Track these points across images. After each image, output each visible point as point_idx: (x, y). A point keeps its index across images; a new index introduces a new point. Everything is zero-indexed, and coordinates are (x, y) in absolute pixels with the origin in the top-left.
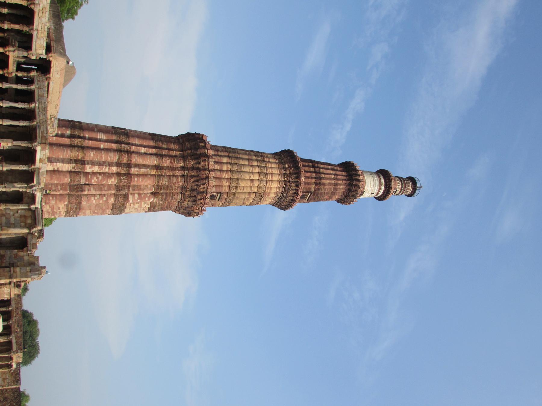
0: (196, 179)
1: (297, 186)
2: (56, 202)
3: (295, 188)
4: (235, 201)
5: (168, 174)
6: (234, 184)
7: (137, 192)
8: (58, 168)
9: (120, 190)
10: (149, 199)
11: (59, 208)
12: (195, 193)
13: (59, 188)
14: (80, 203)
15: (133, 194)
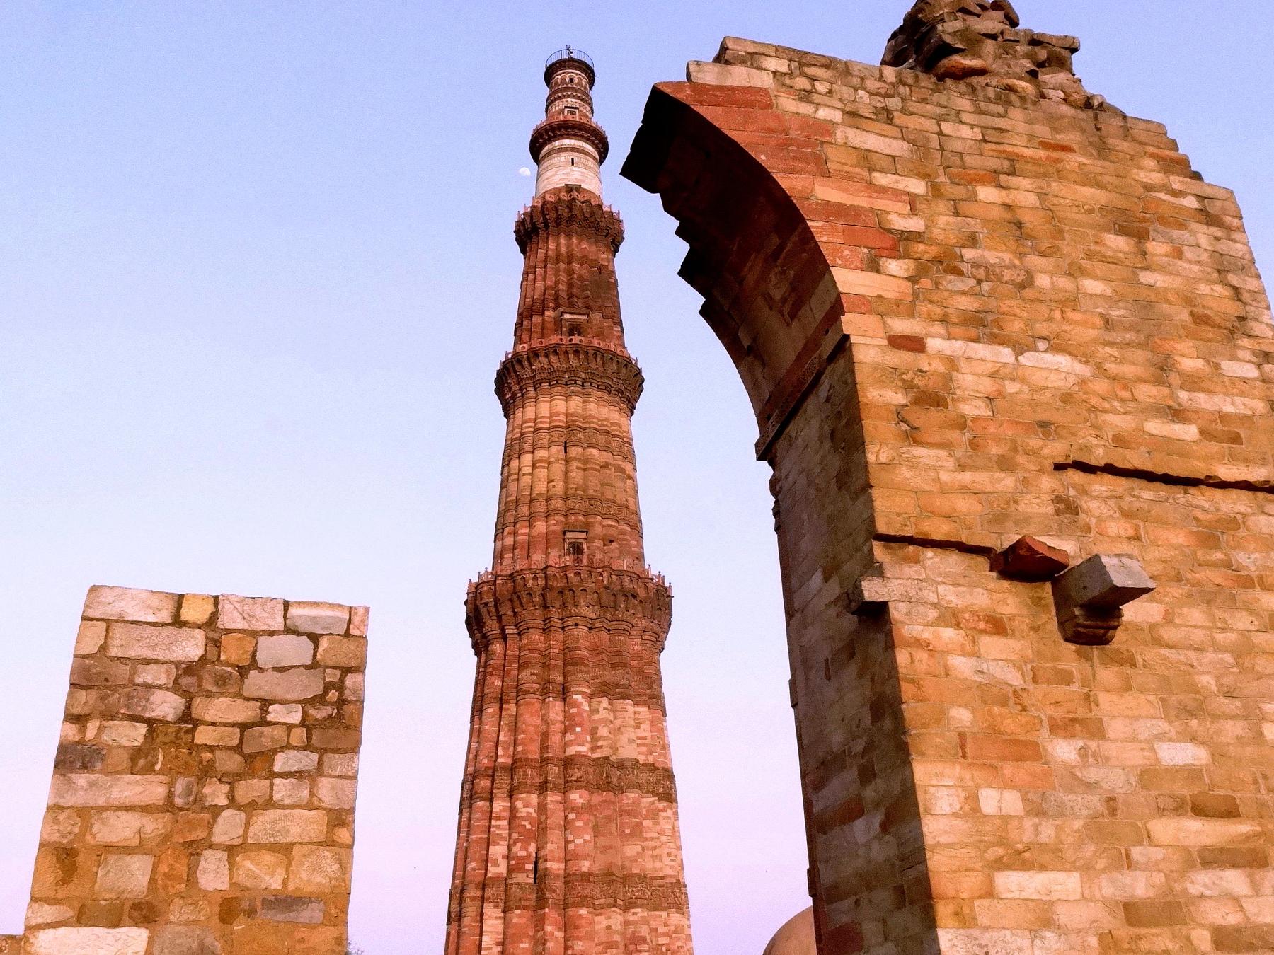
0: (517, 603)
1: (537, 355)
2: (579, 939)
3: (542, 358)
4: (591, 492)
5: (516, 673)
6: (540, 507)
7: (555, 739)
8: (498, 944)
9: (546, 782)
10: (577, 705)
11: (609, 928)
12: (551, 596)
13: (540, 934)
14: (586, 877)
15: (566, 745)
